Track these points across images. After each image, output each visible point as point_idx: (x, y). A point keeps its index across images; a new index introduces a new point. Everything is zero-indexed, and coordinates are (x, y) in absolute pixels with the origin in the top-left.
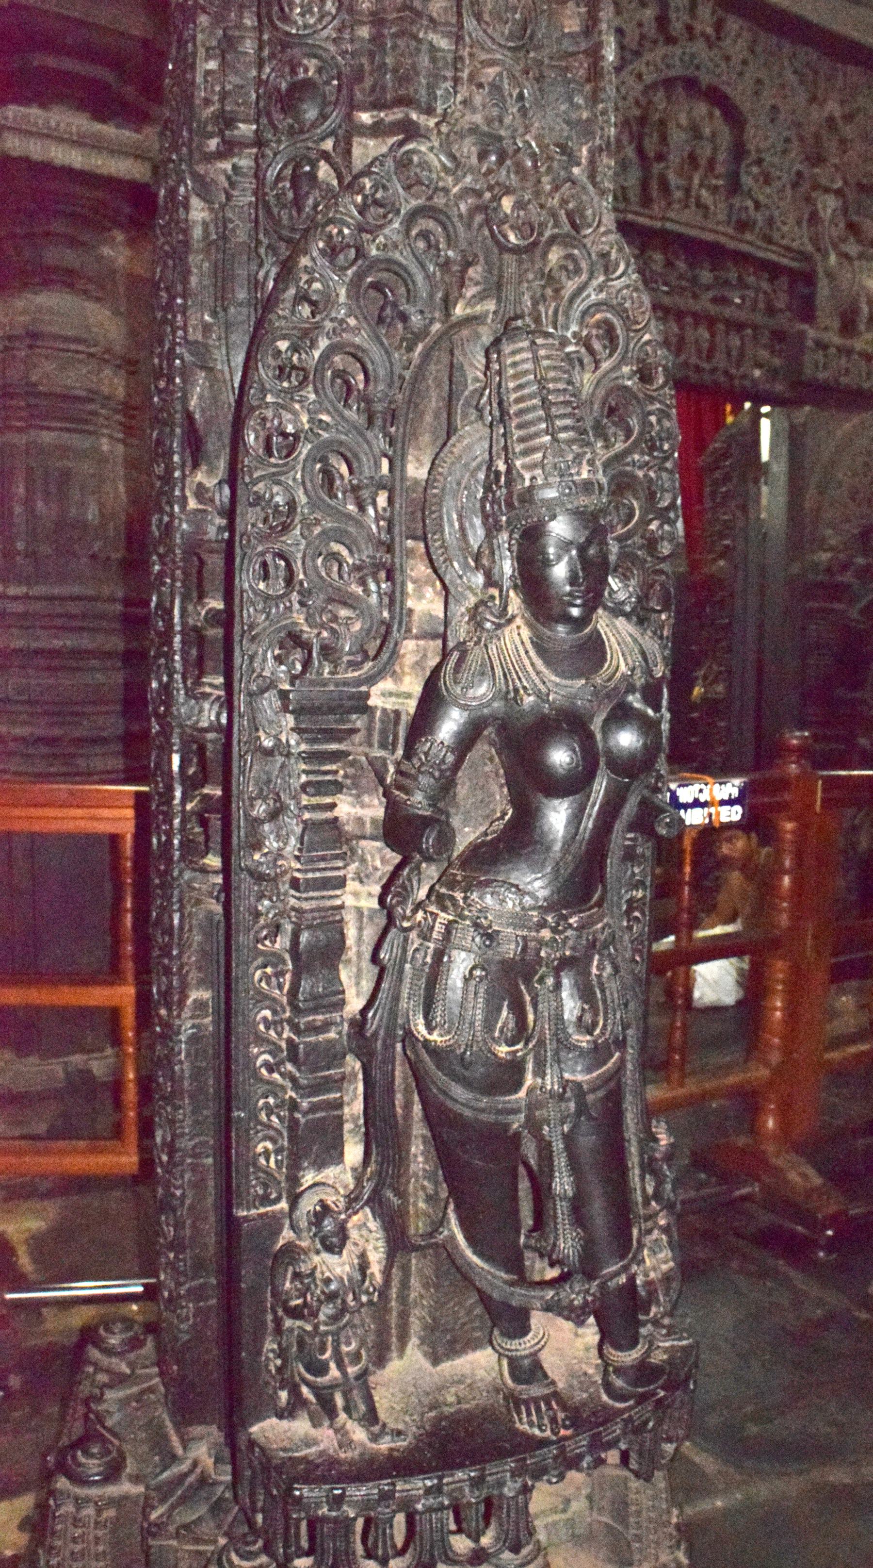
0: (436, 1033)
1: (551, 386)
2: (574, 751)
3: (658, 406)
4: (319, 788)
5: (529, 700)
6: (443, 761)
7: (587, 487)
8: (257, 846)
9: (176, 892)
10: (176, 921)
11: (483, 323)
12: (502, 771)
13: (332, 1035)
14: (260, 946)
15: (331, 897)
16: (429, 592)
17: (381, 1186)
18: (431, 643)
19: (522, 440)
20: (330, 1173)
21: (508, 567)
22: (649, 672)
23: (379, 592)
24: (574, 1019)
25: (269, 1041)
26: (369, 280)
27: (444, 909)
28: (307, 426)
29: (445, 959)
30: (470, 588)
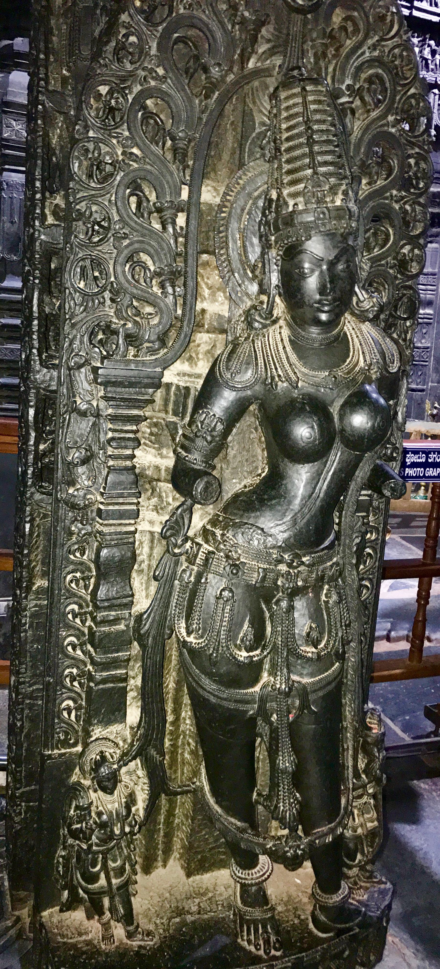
0: (192, 636)
1: (315, 127)
2: (312, 427)
3: (417, 150)
4: (121, 442)
5: (282, 386)
6: (214, 429)
7: (341, 213)
8: (72, 483)
9: (28, 509)
10: (27, 530)
11: (271, 76)
12: (263, 439)
13: (122, 627)
14: (72, 557)
15: (126, 525)
16: (220, 296)
17: (149, 744)
18: (220, 336)
19: (289, 172)
20: (115, 728)
21: (275, 278)
22: (385, 367)
23: (174, 294)
24: (304, 634)
25: (74, 628)
26: (176, 35)
27: (207, 542)
28: (121, 158)
29: (203, 580)
30: (247, 294)
